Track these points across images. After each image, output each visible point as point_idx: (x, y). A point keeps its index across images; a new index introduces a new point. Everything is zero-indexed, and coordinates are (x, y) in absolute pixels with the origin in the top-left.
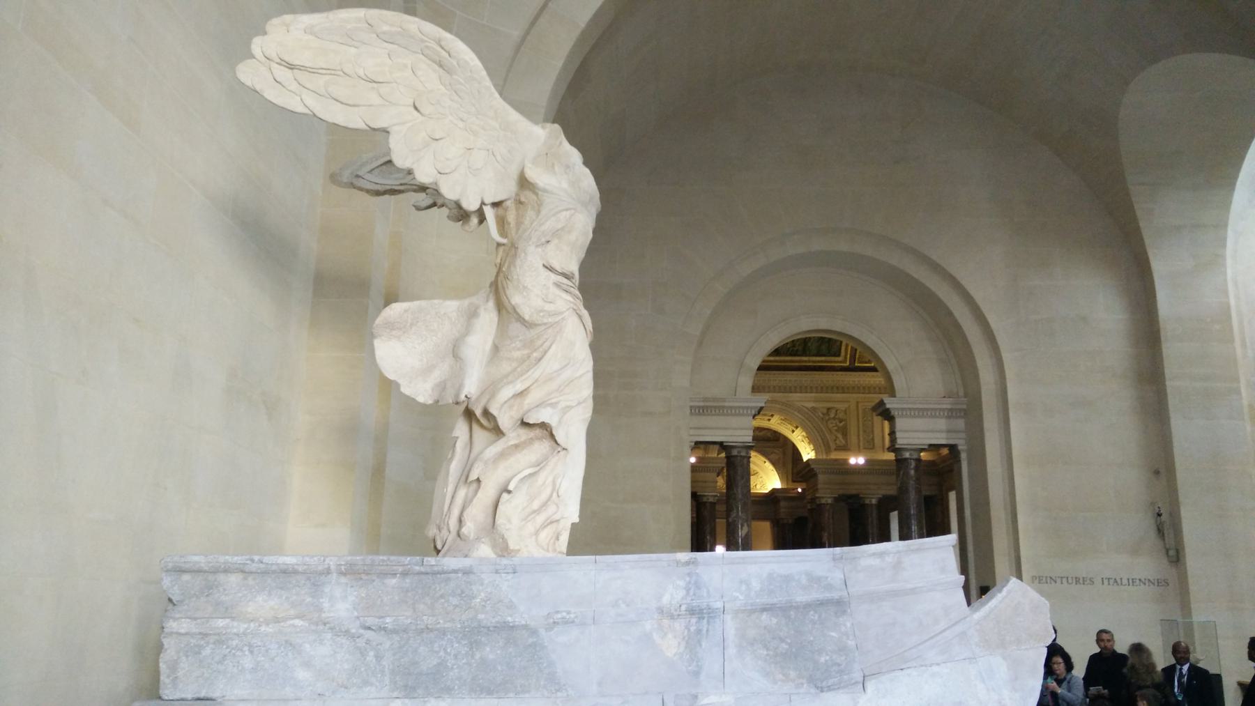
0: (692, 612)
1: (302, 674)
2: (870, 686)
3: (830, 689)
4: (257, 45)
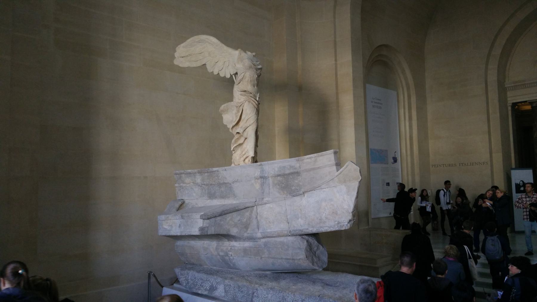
0: (261, 177)
1: (194, 194)
2: (306, 195)
3: (294, 196)
4: (176, 55)
